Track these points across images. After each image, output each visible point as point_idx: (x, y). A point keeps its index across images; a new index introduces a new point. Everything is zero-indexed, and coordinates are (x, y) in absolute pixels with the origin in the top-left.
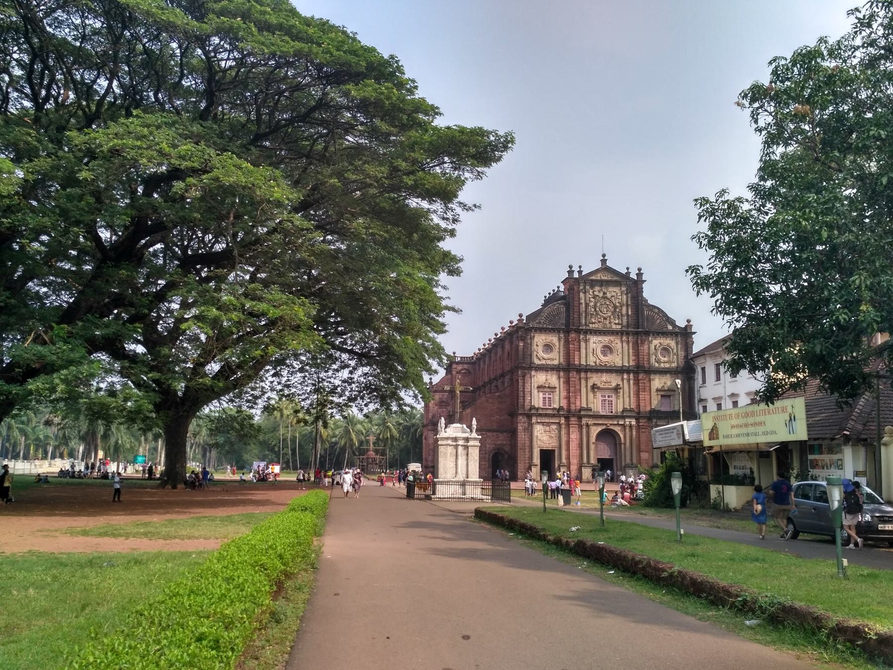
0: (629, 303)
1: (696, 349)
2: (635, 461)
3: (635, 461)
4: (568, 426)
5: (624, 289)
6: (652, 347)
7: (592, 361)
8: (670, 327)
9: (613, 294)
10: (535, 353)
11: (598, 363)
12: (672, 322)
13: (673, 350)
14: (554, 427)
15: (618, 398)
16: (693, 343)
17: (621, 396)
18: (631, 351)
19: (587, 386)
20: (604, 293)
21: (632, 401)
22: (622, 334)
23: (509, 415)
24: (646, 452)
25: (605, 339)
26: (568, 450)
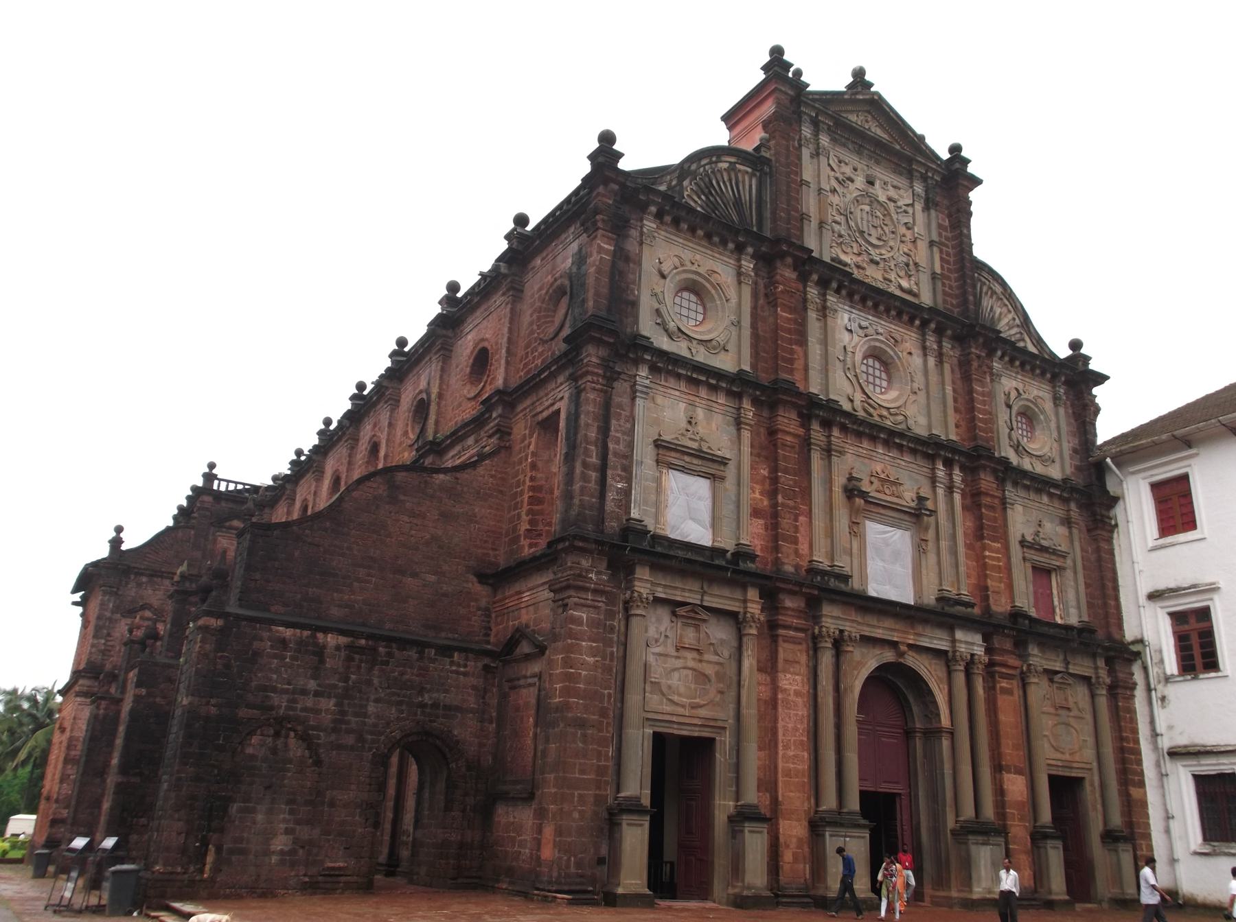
0: (935, 237)
1: (1107, 428)
2: (989, 812)
3: (989, 812)
4: (772, 628)
5: (919, 188)
6: (1001, 399)
7: (841, 391)
9: (892, 193)
11: (857, 404)
12: (1039, 341)
13: (1048, 420)
16: (1097, 410)
17: (931, 545)
18: (949, 389)
19: (829, 482)
20: (871, 183)
21: (962, 569)
22: (924, 324)
23: (482, 578)
24: (1019, 772)
25: (882, 328)
26: (770, 741)
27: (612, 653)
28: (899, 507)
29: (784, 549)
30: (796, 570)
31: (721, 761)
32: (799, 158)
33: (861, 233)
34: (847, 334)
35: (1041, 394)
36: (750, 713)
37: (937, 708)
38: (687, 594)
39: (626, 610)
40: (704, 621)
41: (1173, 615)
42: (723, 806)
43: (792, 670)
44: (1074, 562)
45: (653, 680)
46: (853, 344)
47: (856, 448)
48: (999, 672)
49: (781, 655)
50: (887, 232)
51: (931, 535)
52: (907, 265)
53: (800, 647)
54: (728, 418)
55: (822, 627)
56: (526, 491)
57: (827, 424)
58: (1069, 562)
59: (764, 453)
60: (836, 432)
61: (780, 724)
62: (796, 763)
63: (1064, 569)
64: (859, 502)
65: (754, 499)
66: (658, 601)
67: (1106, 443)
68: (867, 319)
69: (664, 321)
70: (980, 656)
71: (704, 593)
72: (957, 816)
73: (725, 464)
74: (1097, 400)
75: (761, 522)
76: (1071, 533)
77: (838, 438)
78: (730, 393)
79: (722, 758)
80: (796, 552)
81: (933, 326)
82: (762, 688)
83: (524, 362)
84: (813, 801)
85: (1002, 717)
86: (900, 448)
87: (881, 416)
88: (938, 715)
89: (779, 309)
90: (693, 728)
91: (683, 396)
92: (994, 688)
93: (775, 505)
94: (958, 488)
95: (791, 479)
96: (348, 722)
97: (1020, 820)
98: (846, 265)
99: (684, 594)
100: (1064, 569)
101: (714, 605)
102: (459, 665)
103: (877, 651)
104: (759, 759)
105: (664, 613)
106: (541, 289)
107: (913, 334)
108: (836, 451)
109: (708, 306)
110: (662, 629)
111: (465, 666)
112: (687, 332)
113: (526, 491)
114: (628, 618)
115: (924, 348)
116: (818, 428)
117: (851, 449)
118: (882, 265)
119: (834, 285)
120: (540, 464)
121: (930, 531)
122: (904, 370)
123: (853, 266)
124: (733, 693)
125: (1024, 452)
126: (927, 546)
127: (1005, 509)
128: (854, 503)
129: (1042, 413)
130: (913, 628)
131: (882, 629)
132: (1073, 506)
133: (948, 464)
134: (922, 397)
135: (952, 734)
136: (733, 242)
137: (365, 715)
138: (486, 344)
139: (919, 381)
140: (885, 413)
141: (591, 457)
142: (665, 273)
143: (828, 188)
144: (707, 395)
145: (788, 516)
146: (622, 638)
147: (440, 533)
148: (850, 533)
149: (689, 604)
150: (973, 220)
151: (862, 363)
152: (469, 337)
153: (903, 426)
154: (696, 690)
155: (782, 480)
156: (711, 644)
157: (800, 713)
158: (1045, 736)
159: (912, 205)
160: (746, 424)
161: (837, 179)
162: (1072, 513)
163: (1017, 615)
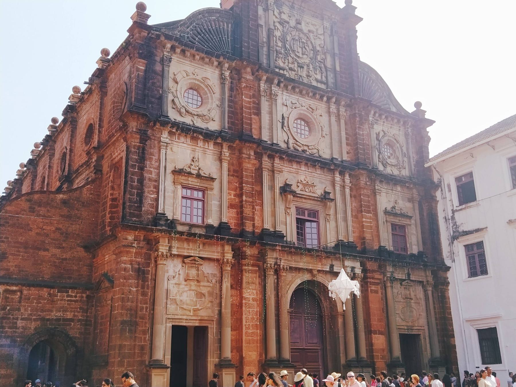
0: (337, 51)
3: (364, 354)
5: (327, 24)
8: (394, 110)
9: (312, 28)
10: (170, 97)
11: (291, 145)
14: (209, 269)
15: (327, 220)
16: (429, 139)
17: (332, 217)
19: (272, 188)
21: (350, 228)
22: (329, 99)
23: (86, 248)
24: (381, 333)
27: (148, 285)
28: (313, 198)
29: (247, 225)
30: (253, 235)
31: (211, 338)
32: (257, 12)
33: (293, 51)
34: (285, 108)
35: (397, 132)
36: (227, 312)
38: (190, 251)
39: (156, 261)
40: (201, 265)
42: (212, 361)
44: (415, 221)
45: (172, 298)
46: (288, 113)
47: (289, 168)
49: (244, 280)
50: (309, 51)
51: (332, 212)
52: (320, 68)
53: (255, 275)
54: (215, 157)
55: (267, 264)
57: (271, 157)
58: (413, 221)
59: (236, 174)
60: (277, 161)
61: (244, 316)
62: (253, 337)
63: (410, 225)
64: (290, 197)
65: (231, 199)
66: (173, 256)
68: (294, 98)
69: (177, 107)
70: (358, 274)
72: (346, 358)
73: (213, 182)
74: (429, 134)
75: (235, 210)
76: (414, 206)
77: (278, 164)
78: (215, 144)
79: (211, 336)
80: (254, 225)
81: (334, 100)
82: (235, 298)
84: (264, 356)
85: (371, 305)
86: (314, 166)
87: (304, 151)
89: (243, 97)
90: (195, 321)
91: (189, 146)
92: (367, 290)
93: (242, 201)
94: (348, 186)
95: (251, 187)
96: (6, 332)
97: (381, 359)
98: (284, 70)
99: (188, 251)
100: (410, 225)
101: (206, 256)
102: (71, 296)
103: (301, 275)
104: (232, 335)
105: (178, 262)
106: (114, 91)
107: (323, 105)
108: (277, 171)
109: (204, 97)
110: (177, 270)
111: (76, 297)
112: (190, 110)
113: (108, 201)
114: (156, 266)
115: (329, 113)
116: (267, 159)
117: (285, 169)
118: (305, 67)
120: (116, 187)
121: (332, 210)
122: (318, 125)
123: (288, 70)
124: (218, 301)
125: (387, 164)
126: (330, 218)
127: (375, 195)
128: (287, 197)
129: (398, 143)
130: (321, 261)
131: (303, 263)
132: (414, 191)
133: (342, 173)
134: (327, 139)
135: (344, 315)
136: (217, 61)
137: (16, 328)
138: (92, 122)
139: (326, 130)
140: (306, 148)
141: (135, 182)
142: (178, 80)
143: (273, 28)
144: (203, 145)
145: (249, 207)
146: (154, 277)
147: (60, 226)
149: (192, 256)
150: (357, 40)
151: (294, 123)
152: (84, 118)
153: (317, 155)
154: (196, 301)
155: (245, 188)
156: (205, 277)
157: (255, 310)
158: (398, 314)
159: (324, 34)
160: (224, 159)
161: (279, 23)
162: (414, 195)
163: (382, 250)
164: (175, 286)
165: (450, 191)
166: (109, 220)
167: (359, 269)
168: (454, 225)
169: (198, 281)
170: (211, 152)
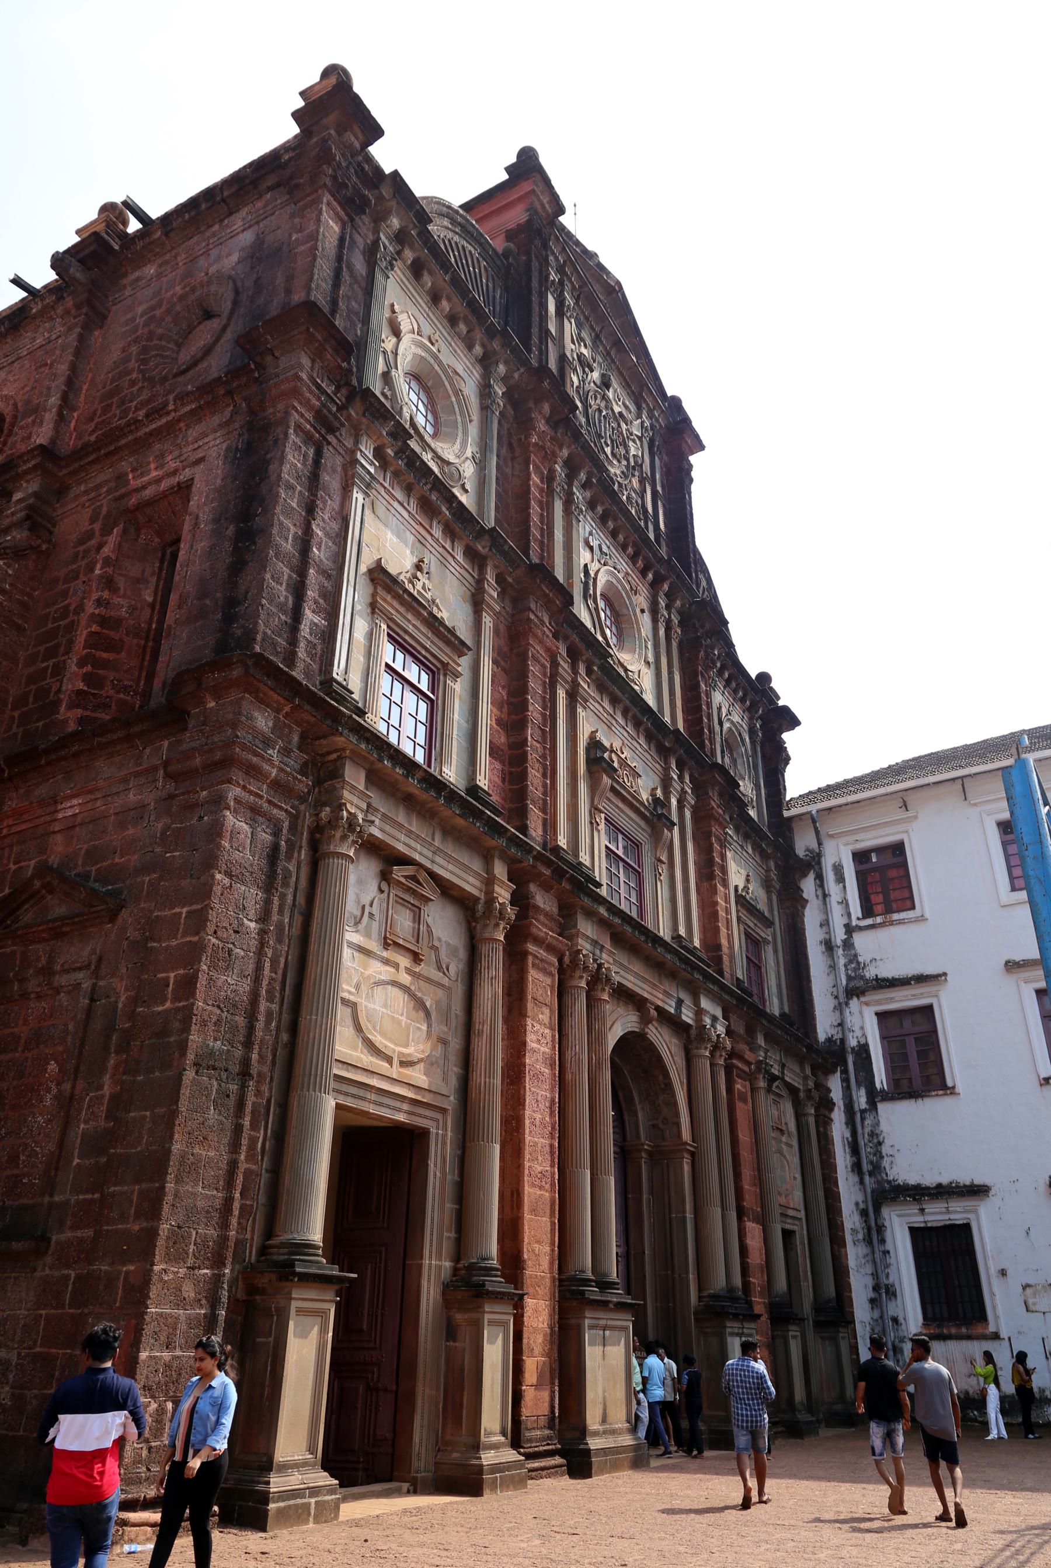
16: (787, 760)
37: (677, 1115)
38: (413, 844)
41: (881, 1016)
43: (541, 1016)
45: (346, 995)
48: (738, 1068)
56: (83, 623)
59: (503, 663)
61: (528, 1112)
64: (606, 780)
67: (809, 797)
71: (437, 851)
76: (770, 899)
83: (97, 420)
88: (678, 1125)
109: (443, 418)
110: (366, 900)
119: (583, 476)
124: (456, 1044)
128: (600, 779)
132: (772, 865)
146: (301, 900)
148: (591, 823)
164: (356, 954)
165: (840, 879)
166: (81, 686)
167: (723, 1025)
168: (851, 962)
169: (416, 958)
170: (458, 568)
